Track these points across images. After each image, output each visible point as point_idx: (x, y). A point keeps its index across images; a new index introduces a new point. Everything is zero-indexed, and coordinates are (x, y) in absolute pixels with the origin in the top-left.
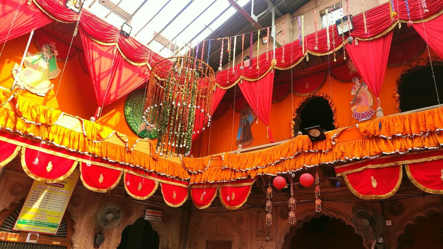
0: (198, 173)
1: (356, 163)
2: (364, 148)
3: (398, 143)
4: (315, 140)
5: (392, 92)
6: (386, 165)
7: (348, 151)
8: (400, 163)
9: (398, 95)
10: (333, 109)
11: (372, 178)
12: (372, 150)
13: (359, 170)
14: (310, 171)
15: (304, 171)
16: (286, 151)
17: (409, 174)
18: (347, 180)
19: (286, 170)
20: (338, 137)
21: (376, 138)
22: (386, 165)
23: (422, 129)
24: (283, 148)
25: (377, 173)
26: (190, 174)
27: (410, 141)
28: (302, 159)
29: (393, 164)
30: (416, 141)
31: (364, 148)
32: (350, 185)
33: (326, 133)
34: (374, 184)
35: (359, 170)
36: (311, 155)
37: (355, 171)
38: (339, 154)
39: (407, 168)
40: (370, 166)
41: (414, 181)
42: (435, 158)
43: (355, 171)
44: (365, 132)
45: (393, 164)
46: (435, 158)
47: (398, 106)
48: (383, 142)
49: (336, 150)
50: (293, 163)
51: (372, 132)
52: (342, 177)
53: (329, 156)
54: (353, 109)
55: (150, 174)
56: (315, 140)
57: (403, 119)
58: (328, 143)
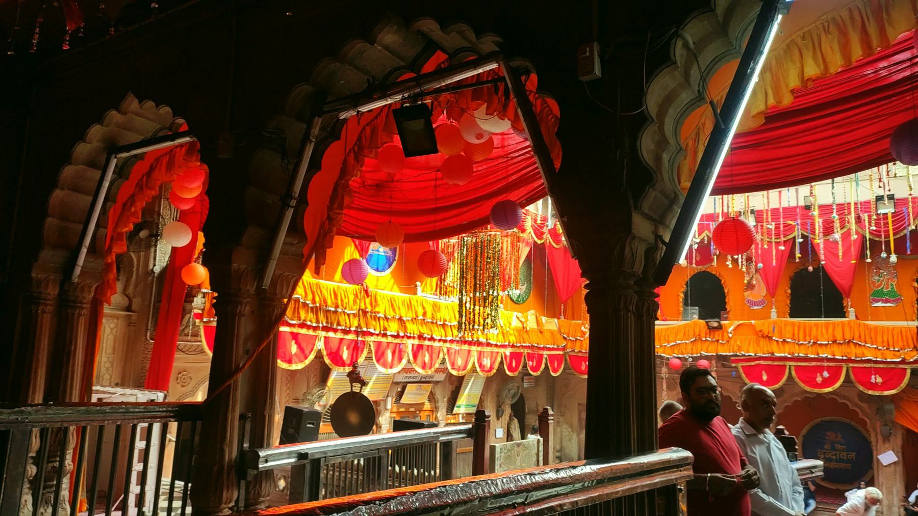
0: (576, 339)
1: (750, 359)
2: (758, 344)
3: (787, 347)
4: (711, 329)
5: (784, 290)
6: (776, 363)
7: (745, 347)
8: (788, 363)
9: (789, 291)
10: (726, 291)
11: (764, 372)
12: (766, 349)
13: (753, 363)
14: (706, 358)
15: (701, 357)
16: (681, 335)
17: (793, 373)
18: (741, 371)
19: (682, 354)
20: (734, 330)
21: (770, 338)
22: (776, 363)
23: (808, 338)
24: (678, 329)
25: (768, 368)
26: (565, 338)
27: (797, 347)
28: (699, 345)
29: (782, 363)
30: (802, 347)
31: (758, 344)
32: (743, 375)
33: (723, 322)
34: (765, 378)
35: (753, 363)
36: (708, 343)
37: (748, 364)
38: (736, 348)
39: (793, 368)
40: (762, 362)
41: (797, 380)
42: (813, 364)
43: (748, 364)
44: (761, 331)
45: (782, 363)
46: (813, 364)
47: (788, 310)
48: (775, 343)
49: (732, 342)
50: (690, 347)
51: (766, 333)
52: (736, 367)
53: (726, 347)
54: (746, 294)
55: (539, 348)
56: (711, 329)
57: (793, 324)
58: (725, 334)
